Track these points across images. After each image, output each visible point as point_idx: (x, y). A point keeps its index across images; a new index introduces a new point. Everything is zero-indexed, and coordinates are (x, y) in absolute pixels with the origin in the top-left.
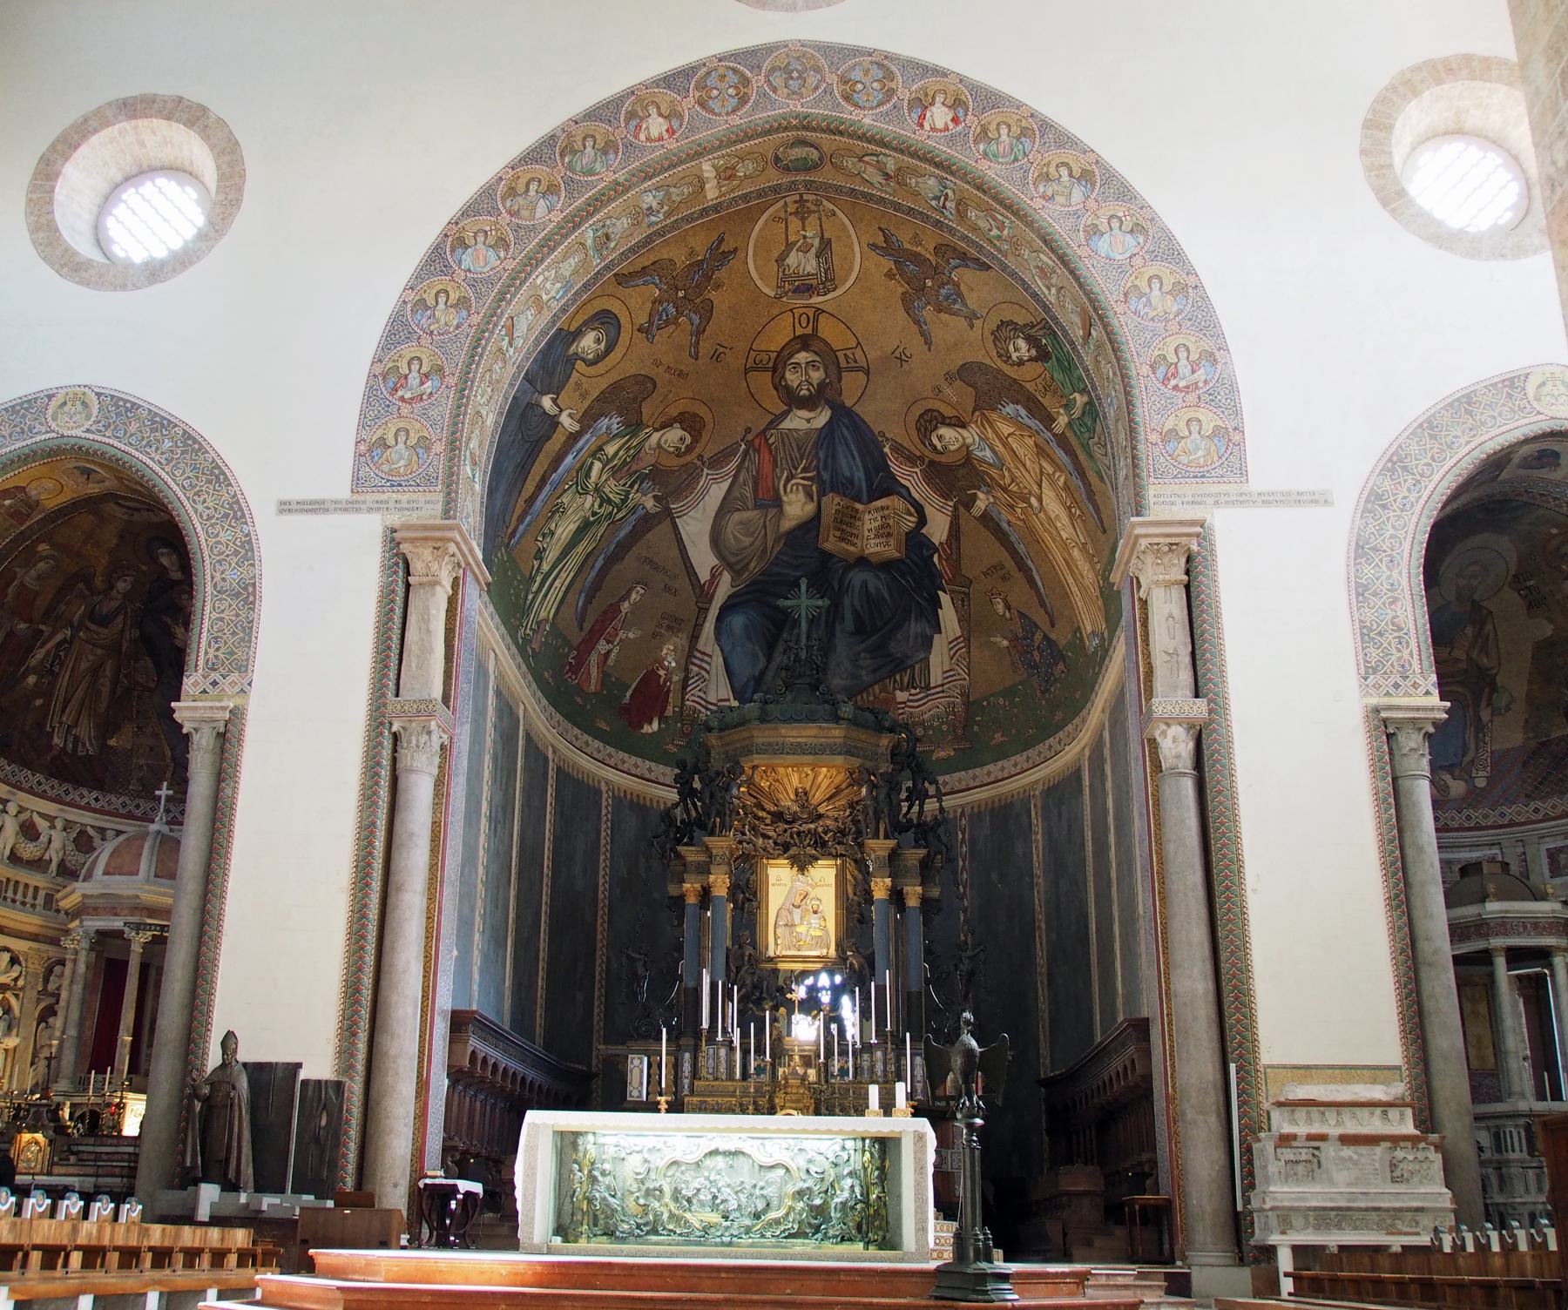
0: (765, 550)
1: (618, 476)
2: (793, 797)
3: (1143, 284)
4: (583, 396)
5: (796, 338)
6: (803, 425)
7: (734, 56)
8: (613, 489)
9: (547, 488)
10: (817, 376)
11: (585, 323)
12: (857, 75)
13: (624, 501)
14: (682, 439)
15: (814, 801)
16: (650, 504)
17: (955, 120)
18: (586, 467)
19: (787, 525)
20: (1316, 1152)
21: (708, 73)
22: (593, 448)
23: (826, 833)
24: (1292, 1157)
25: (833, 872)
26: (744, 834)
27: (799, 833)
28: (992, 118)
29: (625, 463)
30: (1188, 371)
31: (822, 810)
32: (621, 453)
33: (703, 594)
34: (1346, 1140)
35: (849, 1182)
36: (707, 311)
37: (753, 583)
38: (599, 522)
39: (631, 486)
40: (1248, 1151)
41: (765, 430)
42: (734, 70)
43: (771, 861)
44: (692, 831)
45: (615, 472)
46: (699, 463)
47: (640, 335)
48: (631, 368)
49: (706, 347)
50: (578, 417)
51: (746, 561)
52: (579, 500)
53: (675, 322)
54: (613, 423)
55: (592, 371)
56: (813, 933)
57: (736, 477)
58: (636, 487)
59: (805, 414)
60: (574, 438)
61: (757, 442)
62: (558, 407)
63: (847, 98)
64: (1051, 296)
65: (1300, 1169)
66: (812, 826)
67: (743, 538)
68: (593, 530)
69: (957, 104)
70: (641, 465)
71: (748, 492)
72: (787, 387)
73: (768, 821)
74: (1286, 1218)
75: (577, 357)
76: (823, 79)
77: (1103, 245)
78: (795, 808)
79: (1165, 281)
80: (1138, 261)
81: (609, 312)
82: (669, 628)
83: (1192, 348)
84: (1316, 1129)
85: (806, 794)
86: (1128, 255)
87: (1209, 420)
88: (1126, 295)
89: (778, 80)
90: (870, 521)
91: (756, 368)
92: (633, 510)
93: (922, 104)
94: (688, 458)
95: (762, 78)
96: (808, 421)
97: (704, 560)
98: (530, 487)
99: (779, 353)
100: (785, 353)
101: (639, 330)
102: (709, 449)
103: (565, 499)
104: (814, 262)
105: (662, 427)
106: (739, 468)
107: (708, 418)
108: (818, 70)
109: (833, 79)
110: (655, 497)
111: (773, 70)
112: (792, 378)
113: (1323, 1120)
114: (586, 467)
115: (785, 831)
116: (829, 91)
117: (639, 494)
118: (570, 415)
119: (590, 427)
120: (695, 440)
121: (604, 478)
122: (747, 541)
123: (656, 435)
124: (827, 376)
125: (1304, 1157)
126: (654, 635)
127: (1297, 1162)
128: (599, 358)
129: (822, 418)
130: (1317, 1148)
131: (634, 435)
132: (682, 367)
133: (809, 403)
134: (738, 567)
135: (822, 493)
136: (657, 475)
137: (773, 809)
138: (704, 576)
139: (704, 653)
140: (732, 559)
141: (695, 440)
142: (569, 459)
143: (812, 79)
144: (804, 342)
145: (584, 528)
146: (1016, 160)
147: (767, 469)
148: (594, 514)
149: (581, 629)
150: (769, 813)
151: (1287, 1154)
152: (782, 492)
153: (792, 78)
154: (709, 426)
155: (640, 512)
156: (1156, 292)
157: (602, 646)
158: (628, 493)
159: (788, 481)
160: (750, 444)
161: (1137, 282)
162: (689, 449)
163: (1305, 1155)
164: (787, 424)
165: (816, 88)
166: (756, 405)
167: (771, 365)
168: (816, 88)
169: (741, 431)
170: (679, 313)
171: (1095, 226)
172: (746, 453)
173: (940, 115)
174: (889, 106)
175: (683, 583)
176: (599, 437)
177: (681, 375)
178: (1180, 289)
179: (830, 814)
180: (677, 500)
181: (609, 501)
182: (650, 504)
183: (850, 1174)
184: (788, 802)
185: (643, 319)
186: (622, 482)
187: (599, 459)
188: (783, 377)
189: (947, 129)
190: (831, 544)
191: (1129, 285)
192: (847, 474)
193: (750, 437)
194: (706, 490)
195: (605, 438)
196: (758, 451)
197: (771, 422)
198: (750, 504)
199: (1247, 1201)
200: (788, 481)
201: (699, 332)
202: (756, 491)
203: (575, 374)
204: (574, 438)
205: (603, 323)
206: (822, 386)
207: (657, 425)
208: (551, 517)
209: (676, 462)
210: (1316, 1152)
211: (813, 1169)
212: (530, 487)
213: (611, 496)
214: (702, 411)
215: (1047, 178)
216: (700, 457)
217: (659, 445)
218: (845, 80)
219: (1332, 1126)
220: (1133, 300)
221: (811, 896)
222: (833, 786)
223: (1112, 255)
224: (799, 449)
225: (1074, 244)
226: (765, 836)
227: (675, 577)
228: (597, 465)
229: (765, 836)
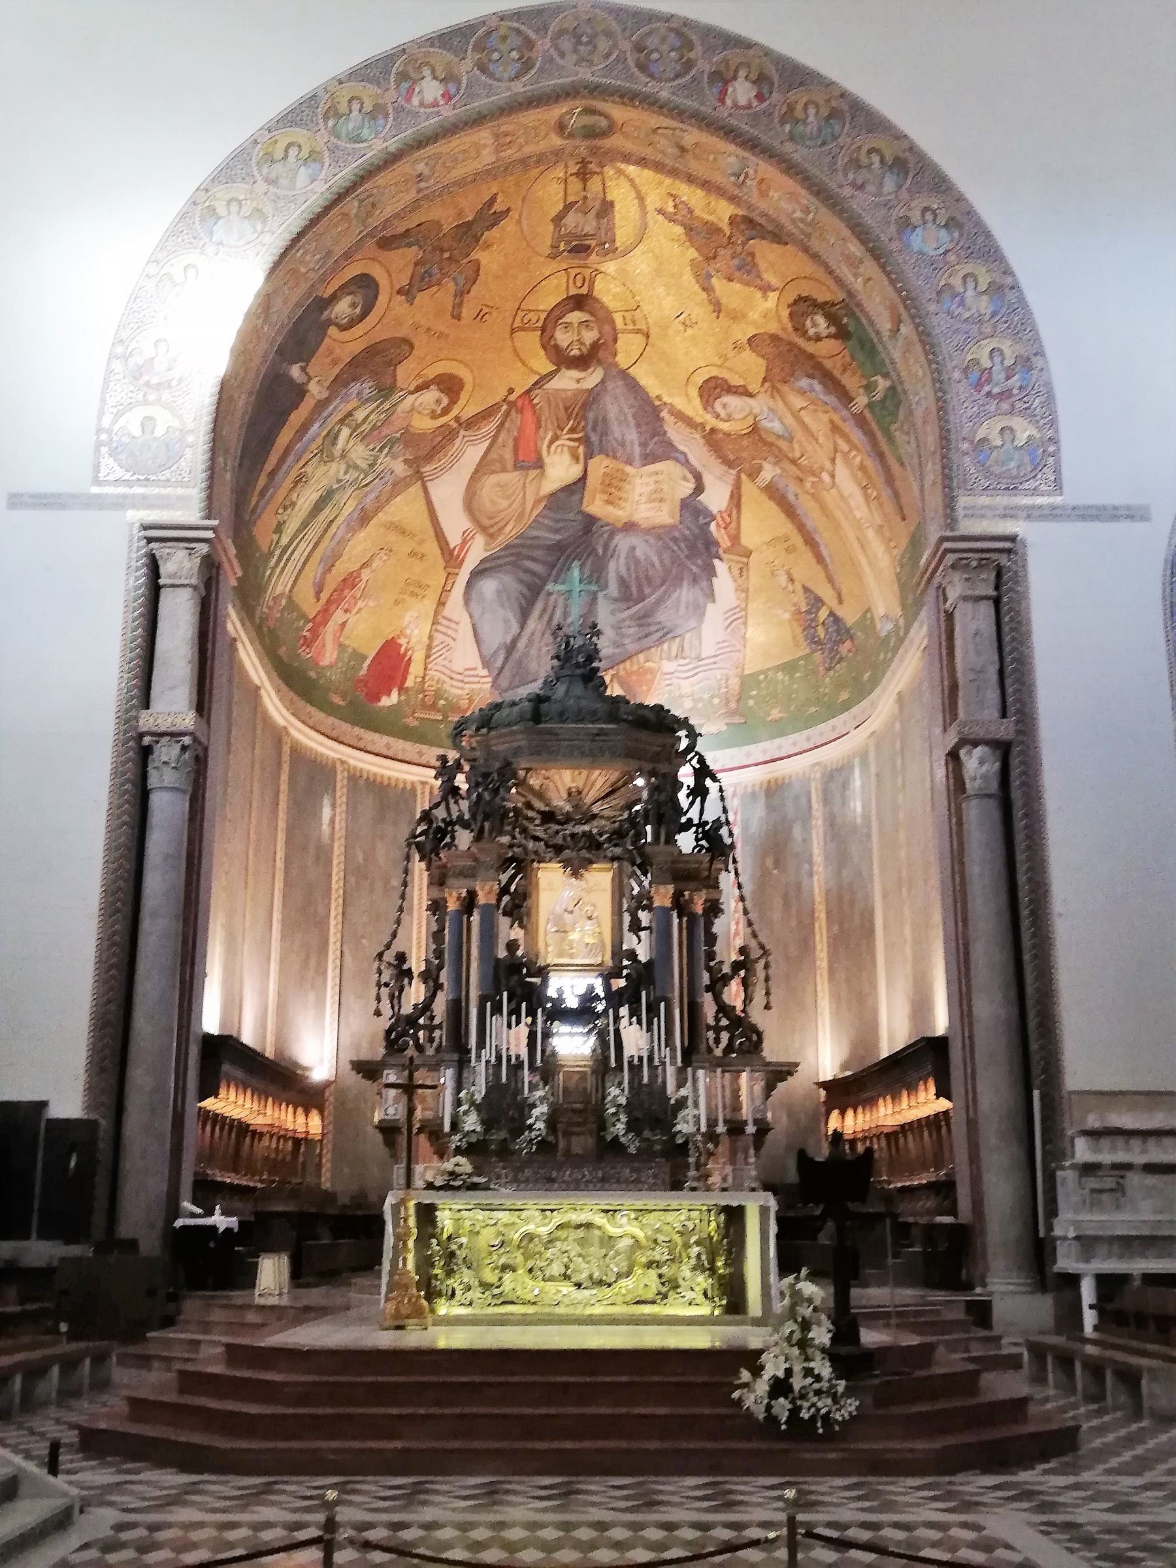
0: (521, 515)
2: (565, 796)
3: (956, 281)
6: (573, 386)
7: (518, 15)
10: (590, 336)
12: (652, 42)
15: (588, 800)
17: (760, 97)
20: (1121, 1181)
21: (489, 33)
23: (601, 835)
24: (1097, 1186)
25: (609, 876)
26: (514, 838)
27: (573, 835)
28: (799, 97)
30: (1002, 376)
31: (596, 809)
33: (452, 559)
34: (1151, 1168)
35: (695, 1250)
40: (1050, 1179)
41: (528, 392)
42: (518, 32)
43: (542, 865)
44: (453, 831)
56: (587, 940)
57: (495, 438)
59: (575, 374)
61: (520, 403)
63: (642, 67)
64: (858, 285)
65: (1105, 1197)
66: (586, 828)
69: (761, 80)
71: (508, 456)
72: (556, 347)
73: (537, 822)
74: (1088, 1244)
76: (615, 46)
77: (917, 240)
78: (568, 808)
79: (981, 280)
80: (952, 258)
82: (413, 594)
83: (1007, 352)
84: (1121, 1157)
85: (580, 793)
86: (941, 250)
87: (1024, 431)
88: (939, 293)
89: (566, 44)
93: (722, 79)
95: (548, 40)
96: (578, 381)
97: (455, 524)
100: (556, 313)
104: (595, 224)
108: (609, 34)
109: (626, 46)
110: (405, 461)
111: (562, 32)
112: (563, 338)
113: (1128, 1149)
115: (557, 832)
116: (621, 59)
117: (388, 458)
122: (504, 504)
125: (1108, 1186)
126: (396, 602)
127: (1101, 1191)
130: (1122, 1177)
134: (492, 531)
137: (543, 808)
138: (454, 540)
139: (450, 620)
140: (486, 522)
143: (603, 45)
146: (824, 144)
147: (530, 428)
149: (318, 600)
150: (539, 812)
151: (1092, 1183)
153: (582, 44)
154: (468, 387)
156: (970, 293)
157: (338, 616)
159: (551, 442)
161: (952, 281)
163: (1109, 1183)
164: (555, 384)
165: (608, 55)
166: (520, 365)
167: (540, 324)
168: (608, 55)
169: (503, 393)
171: (908, 218)
172: (507, 414)
173: (742, 91)
174: (688, 78)
175: (432, 548)
178: (996, 290)
179: (603, 813)
183: (697, 1243)
184: (560, 803)
189: (749, 107)
191: (942, 283)
193: (512, 397)
196: (521, 411)
197: (536, 383)
198: (510, 465)
199: (1050, 1228)
200: (551, 442)
202: (516, 451)
206: (595, 346)
210: (1121, 1181)
211: (661, 1238)
215: (855, 164)
218: (639, 48)
219: (1136, 1154)
220: (946, 296)
221: (586, 900)
222: (609, 783)
223: (925, 250)
224: (566, 409)
225: (885, 234)
226: (537, 839)
227: (422, 541)
229: (537, 839)
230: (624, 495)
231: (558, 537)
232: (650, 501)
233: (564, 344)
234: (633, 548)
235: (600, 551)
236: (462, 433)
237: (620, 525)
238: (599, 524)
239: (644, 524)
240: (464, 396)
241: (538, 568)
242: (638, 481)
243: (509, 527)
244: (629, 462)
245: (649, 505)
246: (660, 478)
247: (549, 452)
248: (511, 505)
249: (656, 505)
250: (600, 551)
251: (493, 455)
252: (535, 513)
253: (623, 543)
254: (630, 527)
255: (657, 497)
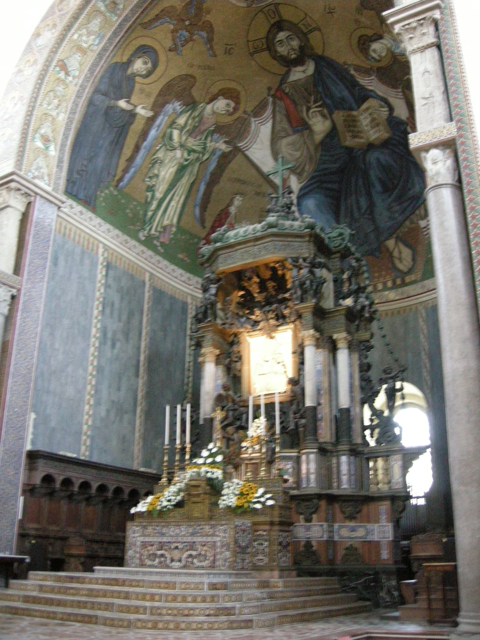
1: (194, 135)
4: (148, 95)
5: (273, 25)
8: (192, 143)
9: (142, 153)
10: (295, 43)
11: (132, 55)
13: (204, 148)
14: (228, 105)
16: (223, 147)
18: (168, 135)
19: (318, 138)
22: (169, 123)
29: (195, 127)
32: (190, 122)
36: (209, 28)
37: (313, 178)
38: (191, 163)
39: (206, 139)
45: (191, 133)
46: (246, 116)
47: (172, 53)
48: (174, 73)
49: (219, 49)
50: (150, 107)
51: (301, 167)
52: (171, 154)
53: (191, 40)
54: (175, 106)
55: (147, 81)
57: (274, 118)
58: (209, 139)
60: (151, 121)
62: (132, 104)
67: (296, 153)
68: (189, 169)
70: (207, 126)
71: (286, 125)
75: (134, 75)
81: (144, 46)
90: (364, 121)
91: (256, 52)
92: (213, 153)
94: (237, 115)
98: (127, 151)
99: (267, 38)
101: (170, 50)
102: (248, 105)
103: (160, 155)
105: (211, 100)
106: (274, 112)
107: (239, 88)
112: (282, 50)
114: (168, 135)
118: (143, 108)
119: (161, 111)
120: (237, 103)
121: (184, 138)
122: (298, 154)
123: (209, 107)
124: (301, 42)
128: (149, 74)
129: (310, 68)
131: (194, 109)
132: (209, 63)
133: (299, 61)
135: (331, 113)
136: (219, 129)
141: (237, 103)
142: (153, 133)
144: (279, 26)
145: (181, 169)
148: (186, 160)
152: (307, 119)
154: (243, 93)
155: (218, 153)
158: (205, 144)
160: (274, 96)
162: (235, 109)
167: (265, 46)
170: (192, 34)
176: (170, 116)
177: (209, 68)
180: (241, 141)
181: (194, 151)
182: (223, 147)
185: (169, 43)
186: (198, 138)
187: (175, 128)
188: (276, 51)
190: (349, 142)
192: (339, 95)
194: (258, 130)
195: (174, 116)
201: (210, 40)
203: (137, 87)
204: (151, 121)
205: (145, 53)
206: (301, 48)
207: (207, 100)
208: (153, 166)
209: (228, 120)
212: (127, 151)
213: (194, 147)
214: (233, 85)
216: (245, 112)
217: (214, 113)
228: (176, 133)
230: (359, 129)
231: (337, 165)
232: (373, 128)
233: (285, 53)
234: (378, 160)
235: (363, 166)
236: (253, 119)
237: (365, 148)
238: (355, 151)
239: (377, 143)
240: (243, 98)
241: (335, 186)
242: (362, 118)
243: (307, 167)
244: (351, 109)
245: (374, 130)
246: (370, 111)
247: (308, 117)
248: (302, 155)
249: (377, 128)
250: (363, 166)
251: (278, 127)
252: (318, 155)
253: (372, 157)
254: (371, 146)
255: (374, 123)
